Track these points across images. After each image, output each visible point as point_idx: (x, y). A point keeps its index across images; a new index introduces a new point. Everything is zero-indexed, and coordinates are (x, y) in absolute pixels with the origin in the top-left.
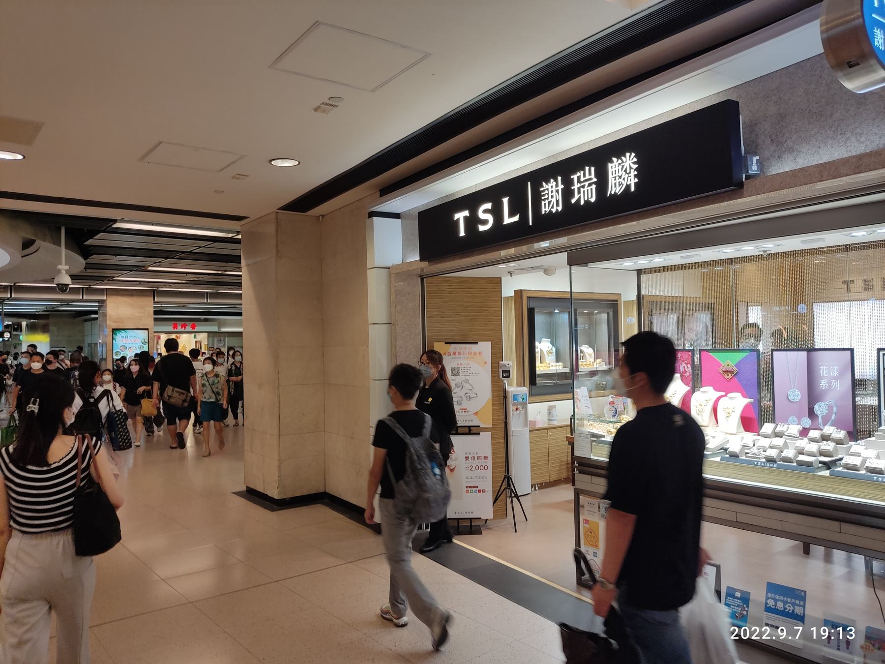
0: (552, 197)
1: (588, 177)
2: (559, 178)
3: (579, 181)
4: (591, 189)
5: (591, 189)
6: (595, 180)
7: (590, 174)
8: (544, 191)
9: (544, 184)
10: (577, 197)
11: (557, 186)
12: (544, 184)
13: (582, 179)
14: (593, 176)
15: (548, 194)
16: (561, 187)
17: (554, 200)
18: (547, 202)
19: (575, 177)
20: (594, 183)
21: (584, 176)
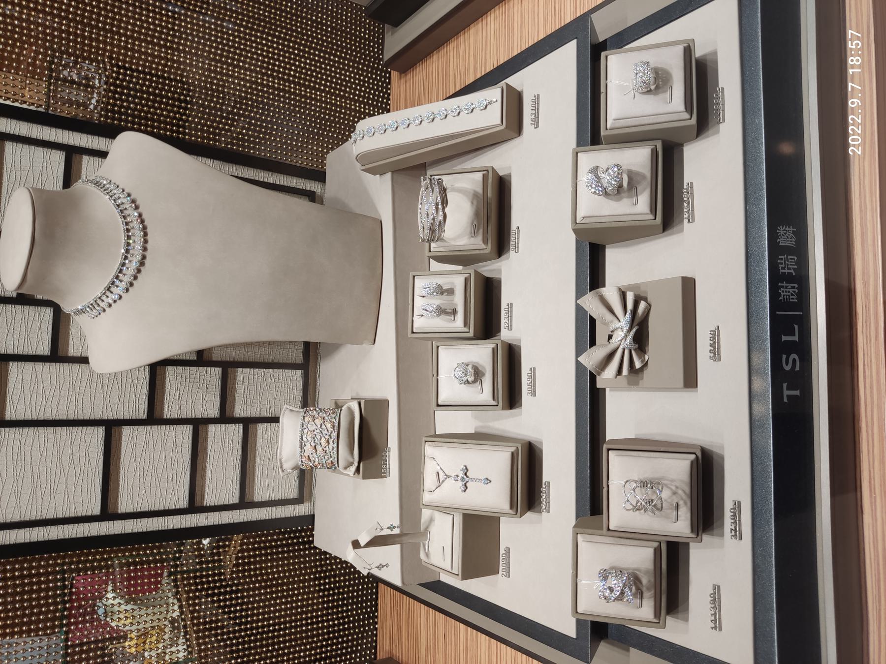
0: (789, 292)
1: (783, 261)
2: (780, 284)
3: (784, 268)
4: (790, 259)
5: (790, 259)
6: (785, 256)
7: (782, 259)
8: (784, 298)
9: (781, 298)
10: (792, 271)
11: (783, 287)
12: (781, 298)
13: (783, 266)
14: (783, 257)
15: (787, 295)
16: (784, 284)
17: (791, 290)
18: (791, 297)
19: (781, 271)
20: (787, 256)
21: (782, 264)
